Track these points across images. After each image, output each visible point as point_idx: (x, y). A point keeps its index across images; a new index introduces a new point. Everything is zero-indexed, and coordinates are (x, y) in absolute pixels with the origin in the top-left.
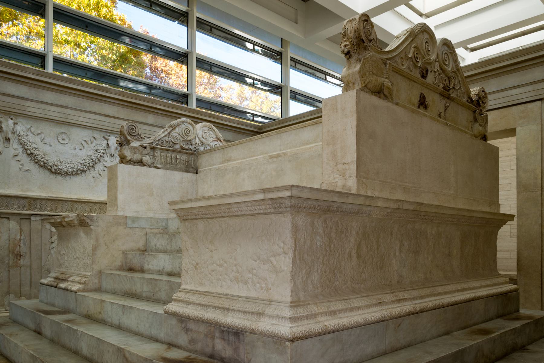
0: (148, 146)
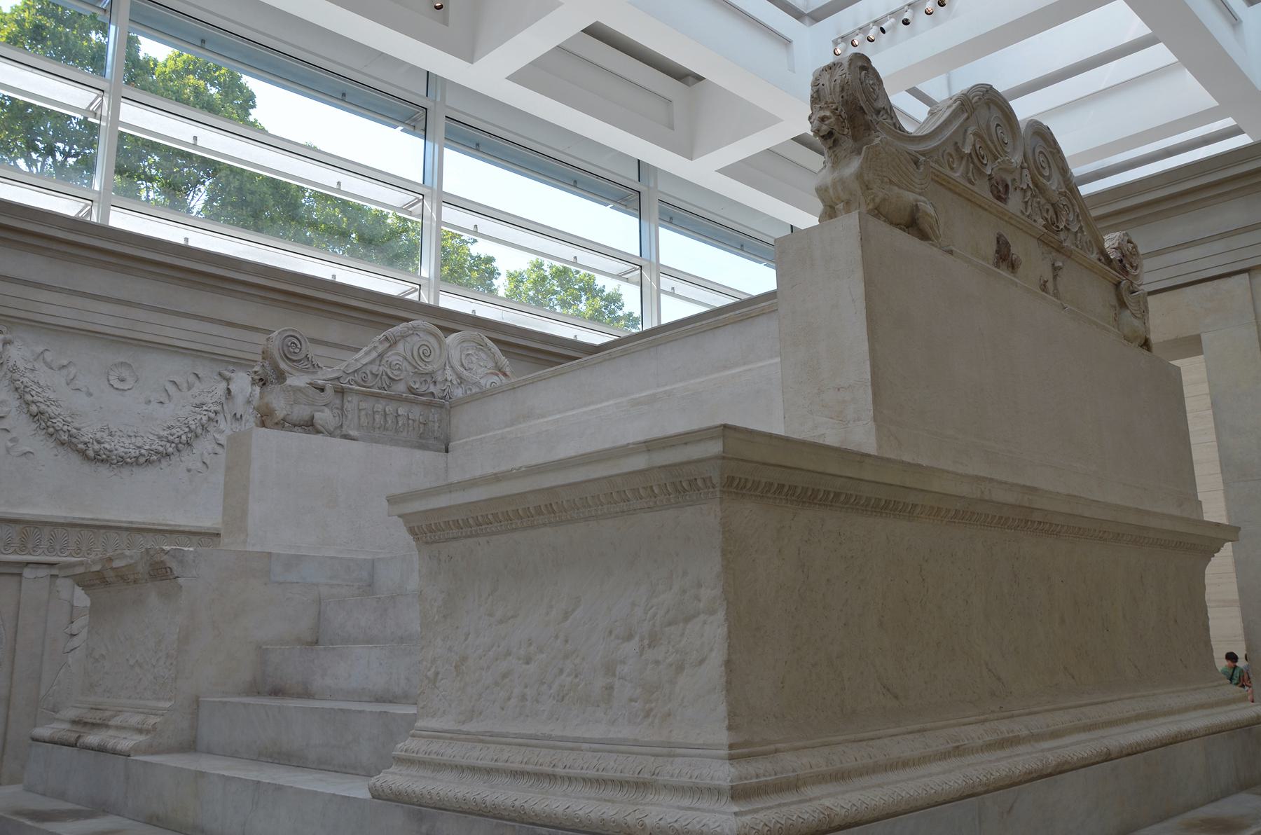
0: (329, 386)
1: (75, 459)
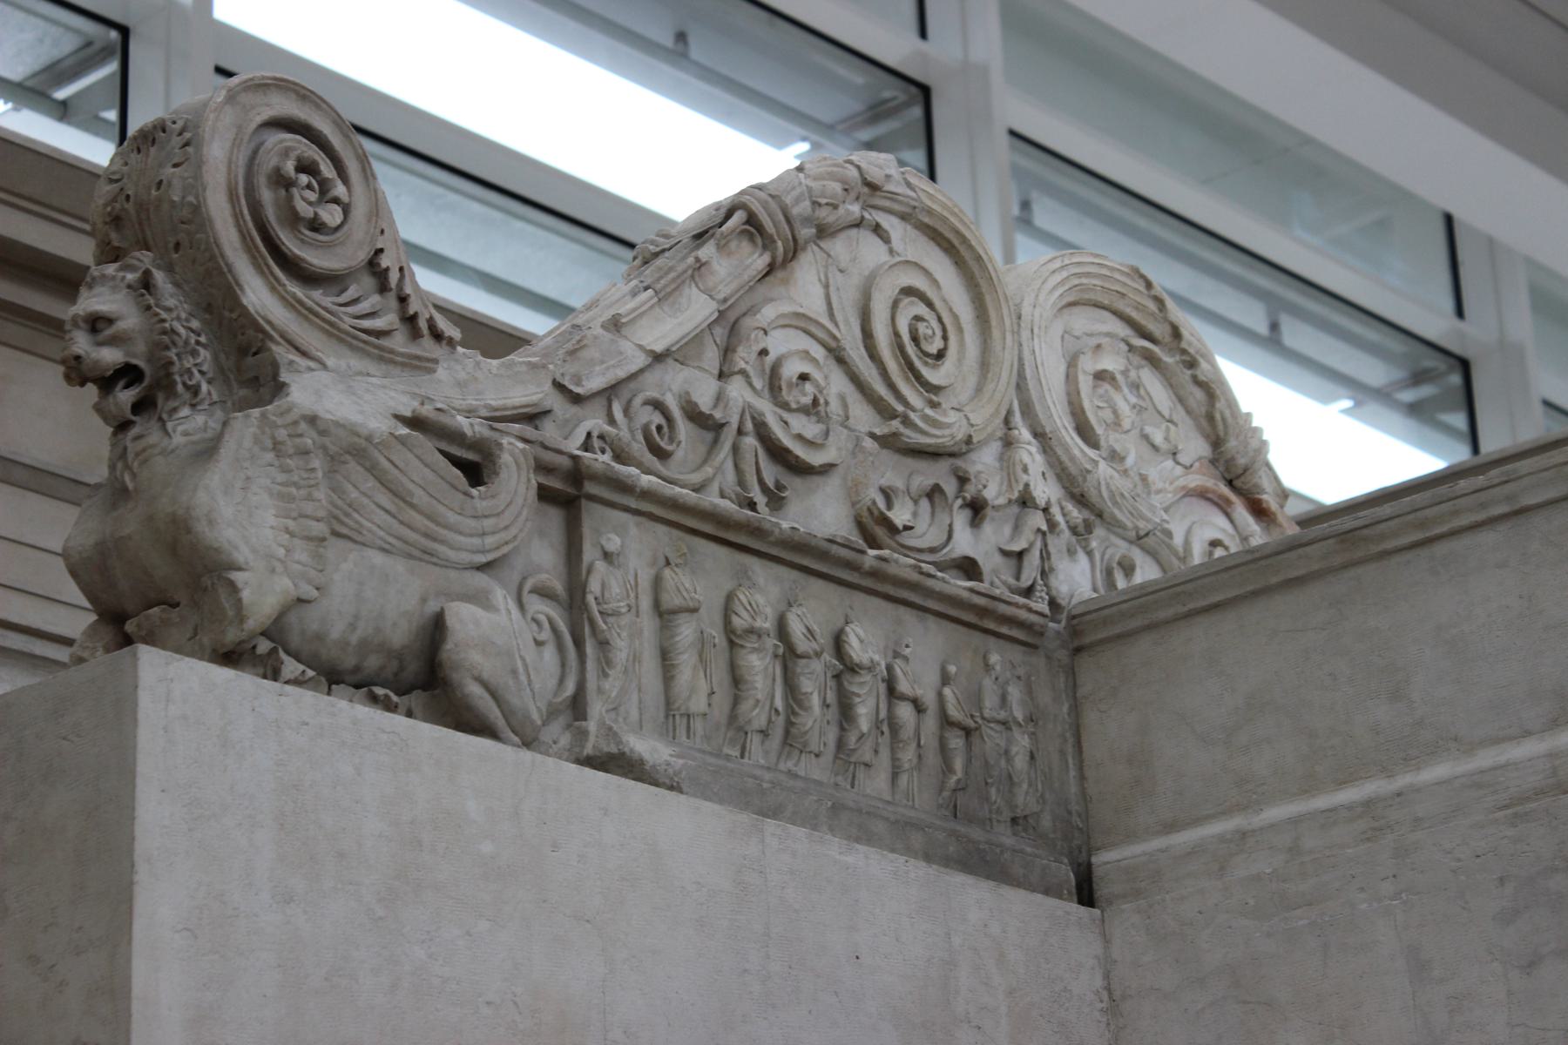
0: (512, 450)
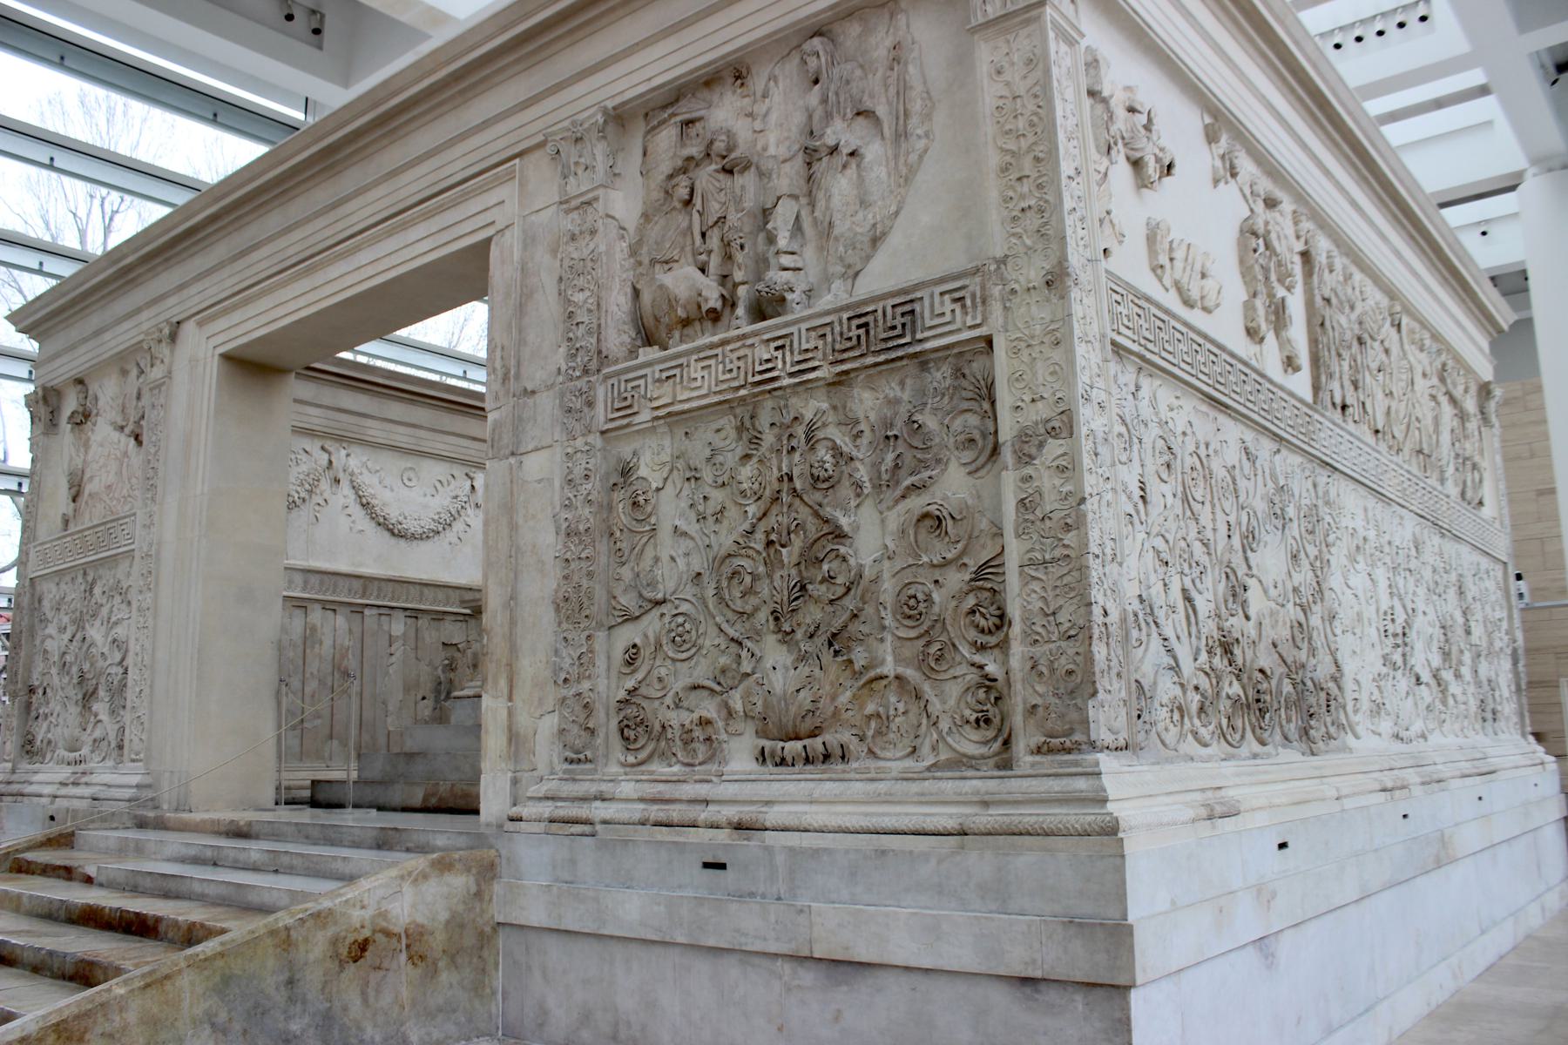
1: (387, 534)
